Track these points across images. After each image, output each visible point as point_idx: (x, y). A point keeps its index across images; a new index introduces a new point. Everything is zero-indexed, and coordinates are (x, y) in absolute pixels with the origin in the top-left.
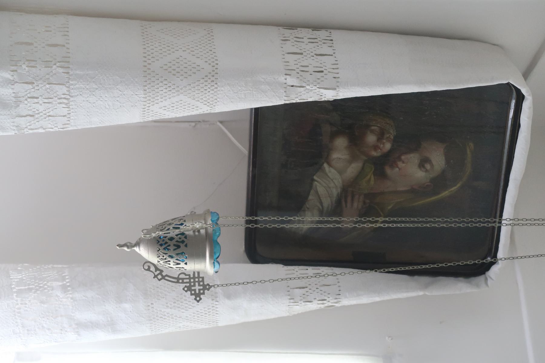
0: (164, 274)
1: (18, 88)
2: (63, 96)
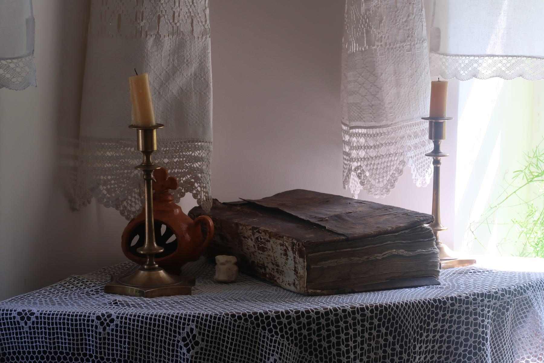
1: (163, 31)
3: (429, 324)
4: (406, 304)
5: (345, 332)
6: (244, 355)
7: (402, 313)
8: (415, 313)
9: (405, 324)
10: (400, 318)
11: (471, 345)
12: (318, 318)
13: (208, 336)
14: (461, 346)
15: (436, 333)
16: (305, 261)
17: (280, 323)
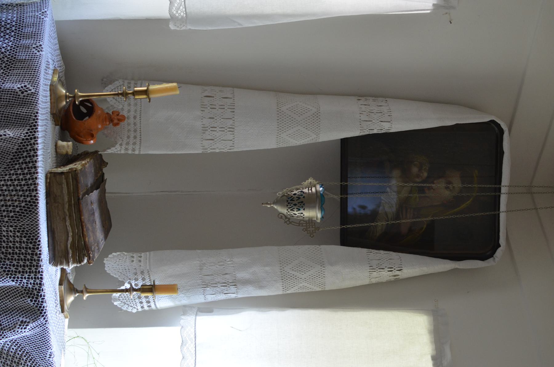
0: (291, 221)
2: (231, 126)
3: (25, 237)
5: (24, 178)
6: (14, 120)
8: (32, 226)
9: (26, 219)
10: (30, 215)
11: (10, 268)
12: (32, 162)
13: (26, 99)
14: (10, 262)
15: (19, 244)
16: (67, 171)
17: (31, 139)
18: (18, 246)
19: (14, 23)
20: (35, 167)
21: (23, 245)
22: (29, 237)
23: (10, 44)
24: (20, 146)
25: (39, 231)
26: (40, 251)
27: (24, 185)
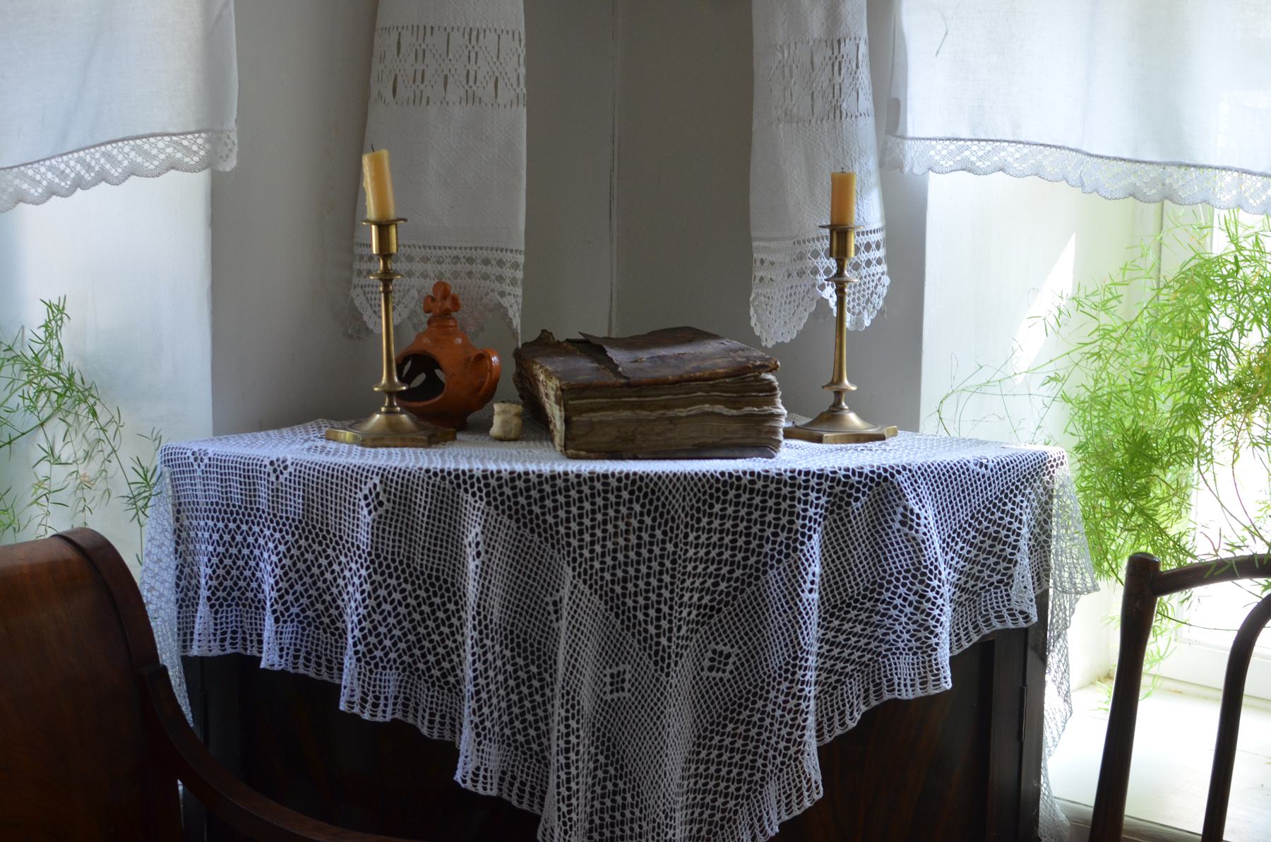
2: (467, 36)
3: (711, 506)
4: (675, 474)
5: (578, 504)
6: (442, 525)
7: (667, 487)
8: (688, 489)
9: (670, 502)
10: (663, 493)
11: (781, 543)
12: (540, 483)
13: (395, 495)
14: (767, 543)
17: (487, 485)
18: (731, 522)
19: (221, 525)
20: (553, 477)
21: (730, 510)
22: (711, 496)
23: (267, 533)
24: (503, 512)
25: (701, 475)
26: (745, 473)
27: (593, 504)
